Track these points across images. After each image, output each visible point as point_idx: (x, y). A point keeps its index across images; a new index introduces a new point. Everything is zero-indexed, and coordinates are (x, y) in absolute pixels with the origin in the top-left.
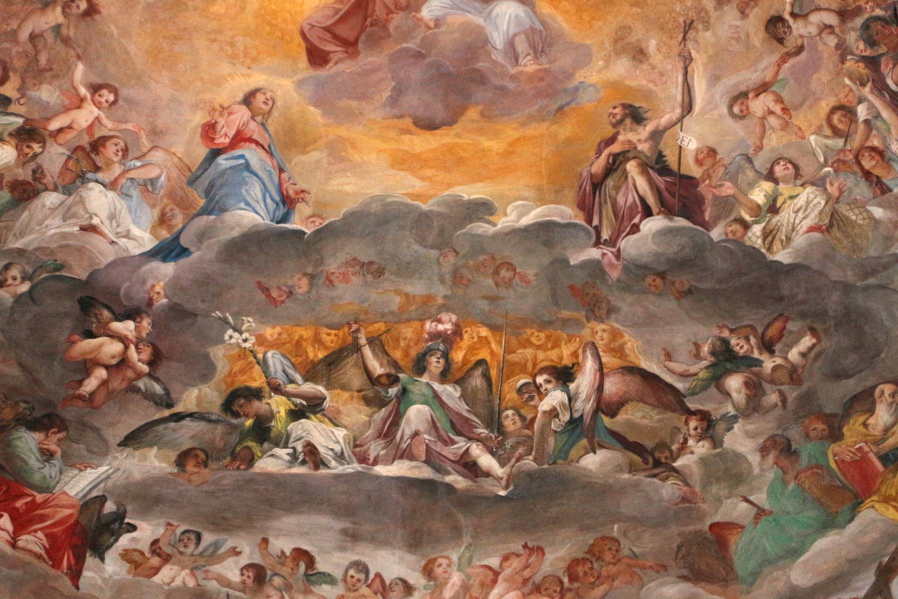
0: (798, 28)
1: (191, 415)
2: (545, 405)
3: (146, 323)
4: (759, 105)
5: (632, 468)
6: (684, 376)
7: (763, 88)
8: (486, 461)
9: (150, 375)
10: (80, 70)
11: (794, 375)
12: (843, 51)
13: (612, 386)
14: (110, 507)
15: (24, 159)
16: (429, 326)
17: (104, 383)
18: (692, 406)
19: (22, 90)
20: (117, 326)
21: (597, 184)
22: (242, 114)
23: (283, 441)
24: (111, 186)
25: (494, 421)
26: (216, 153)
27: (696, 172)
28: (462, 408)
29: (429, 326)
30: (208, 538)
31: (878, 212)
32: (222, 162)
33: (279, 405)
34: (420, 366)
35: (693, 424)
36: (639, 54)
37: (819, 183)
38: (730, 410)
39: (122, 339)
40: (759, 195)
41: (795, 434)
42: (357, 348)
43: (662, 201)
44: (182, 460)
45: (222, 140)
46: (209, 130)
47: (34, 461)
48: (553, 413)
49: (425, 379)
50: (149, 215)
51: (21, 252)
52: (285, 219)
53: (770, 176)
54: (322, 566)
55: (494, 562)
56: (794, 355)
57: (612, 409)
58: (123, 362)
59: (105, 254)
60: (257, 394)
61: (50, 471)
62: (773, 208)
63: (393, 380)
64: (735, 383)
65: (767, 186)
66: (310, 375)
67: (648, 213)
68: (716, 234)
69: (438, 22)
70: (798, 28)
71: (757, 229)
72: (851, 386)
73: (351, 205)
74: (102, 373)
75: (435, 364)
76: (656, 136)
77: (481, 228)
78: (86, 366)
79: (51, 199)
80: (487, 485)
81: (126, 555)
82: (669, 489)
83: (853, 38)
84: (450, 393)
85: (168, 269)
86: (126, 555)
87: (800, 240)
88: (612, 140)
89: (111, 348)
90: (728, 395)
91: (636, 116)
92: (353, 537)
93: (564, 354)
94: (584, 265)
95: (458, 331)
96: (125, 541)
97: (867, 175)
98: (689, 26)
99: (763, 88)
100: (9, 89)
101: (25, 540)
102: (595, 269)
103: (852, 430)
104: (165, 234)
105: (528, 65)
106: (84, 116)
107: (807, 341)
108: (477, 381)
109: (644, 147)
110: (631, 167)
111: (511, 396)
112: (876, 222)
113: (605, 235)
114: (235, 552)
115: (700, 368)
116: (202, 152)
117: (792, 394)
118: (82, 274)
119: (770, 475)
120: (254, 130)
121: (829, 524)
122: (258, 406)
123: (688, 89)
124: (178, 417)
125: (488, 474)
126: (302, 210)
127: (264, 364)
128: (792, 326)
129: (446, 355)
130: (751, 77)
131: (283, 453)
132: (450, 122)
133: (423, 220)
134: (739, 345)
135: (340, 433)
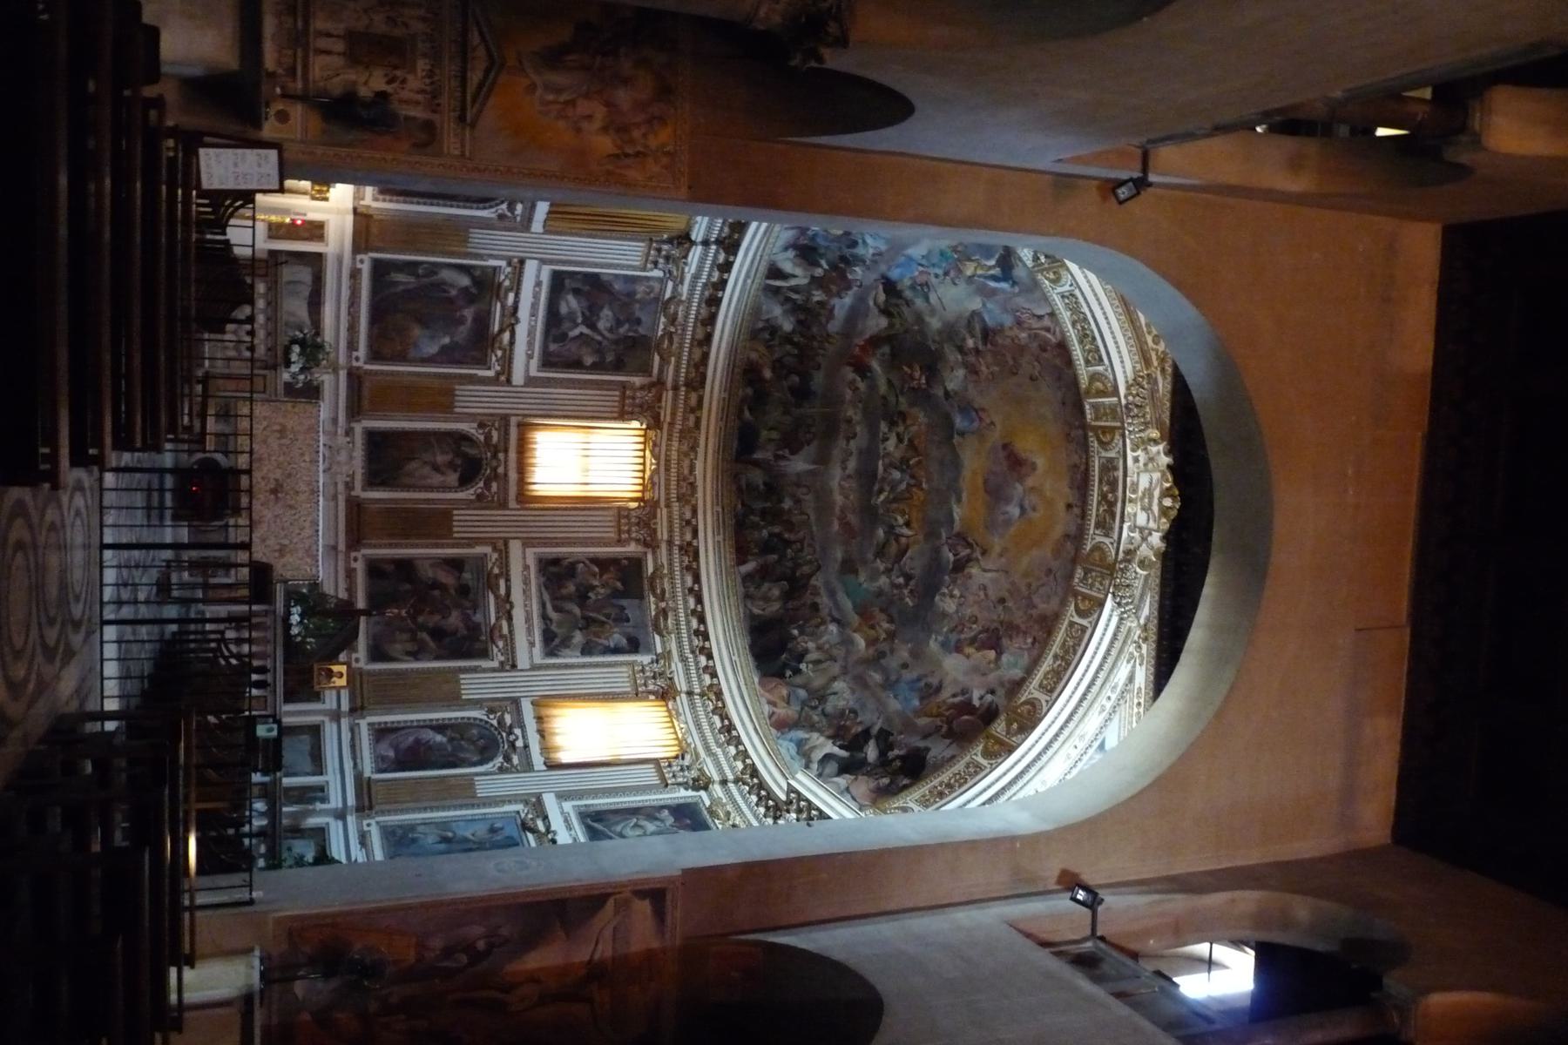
0: (1000, 608)
1: (897, 401)
2: (899, 518)
3: (924, 386)
4: (982, 593)
5: (878, 545)
6: (905, 564)
7: (986, 595)
8: (882, 497)
9: (909, 388)
10: (996, 369)
11: (902, 599)
12: (994, 621)
13: (903, 540)
14: (869, 374)
15: (969, 349)
16: (924, 480)
17: (906, 373)
18: (896, 566)
19: (990, 351)
20: (924, 378)
21: (965, 539)
22: (988, 421)
23: (890, 430)
24: (966, 377)
25: (895, 500)
26: (976, 411)
27: (966, 571)
28: (899, 490)
29: (924, 480)
30: (860, 405)
31: (945, 630)
32: (974, 413)
33: (901, 429)
34: (913, 477)
35: (890, 566)
36: (1001, 555)
37: (957, 612)
38: (893, 577)
39: (919, 380)
40: (956, 592)
41: (884, 598)
42: (918, 456)
43: (958, 560)
44: (884, 398)
45: (980, 413)
46: (983, 410)
47: (881, 351)
48: (896, 520)
49: (908, 477)
50: (956, 388)
51: (943, 348)
52: (958, 434)
53: (961, 596)
54: (852, 442)
55: (851, 497)
56: (907, 599)
57: (897, 541)
58: (912, 378)
59: (946, 374)
60: (904, 421)
61: (878, 356)
62: (952, 596)
63: (908, 466)
64: (901, 580)
65: (958, 595)
66: (910, 440)
67: (955, 555)
68: (947, 578)
69: (1015, 488)
70: (1001, 608)
71: (946, 591)
72: (896, 616)
73: (962, 456)
74: (909, 372)
75: (912, 482)
76: (977, 560)
77: (953, 500)
78: (910, 367)
79: (959, 357)
80: (874, 499)
81: (854, 380)
82: (870, 556)
83: (996, 625)
84: (903, 486)
85: (940, 393)
86: (854, 380)
87: (941, 604)
88: (977, 544)
89: (917, 374)
90: (898, 577)
91: (984, 553)
92: (860, 452)
93: (914, 525)
94: (940, 534)
95: (922, 489)
96: (859, 379)
97: (956, 627)
98: (1007, 572)
99: (986, 595)
100: (989, 346)
101: (857, 349)
102: (939, 537)
103: (883, 616)
104: (952, 393)
105: (1001, 518)
106: (984, 368)
107: (911, 604)
108: (907, 495)
109: (974, 556)
110: (968, 551)
111: (902, 506)
112: (942, 628)
113: (950, 541)
114: (855, 414)
115: (907, 569)
116: (976, 406)
117: (895, 598)
118: (939, 367)
119: (872, 589)
120: (984, 424)
121: (855, 607)
122: (900, 422)
123: (989, 571)
124: (897, 396)
125: (878, 497)
126: (961, 440)
127: (913, 425)
128: (916, 600)
129: (915, 486)
130: (990, 592)
131: (886, 430)
132: (986, 491)
133: (956, 479)
134: (912, 583)
135: (892, 449)
